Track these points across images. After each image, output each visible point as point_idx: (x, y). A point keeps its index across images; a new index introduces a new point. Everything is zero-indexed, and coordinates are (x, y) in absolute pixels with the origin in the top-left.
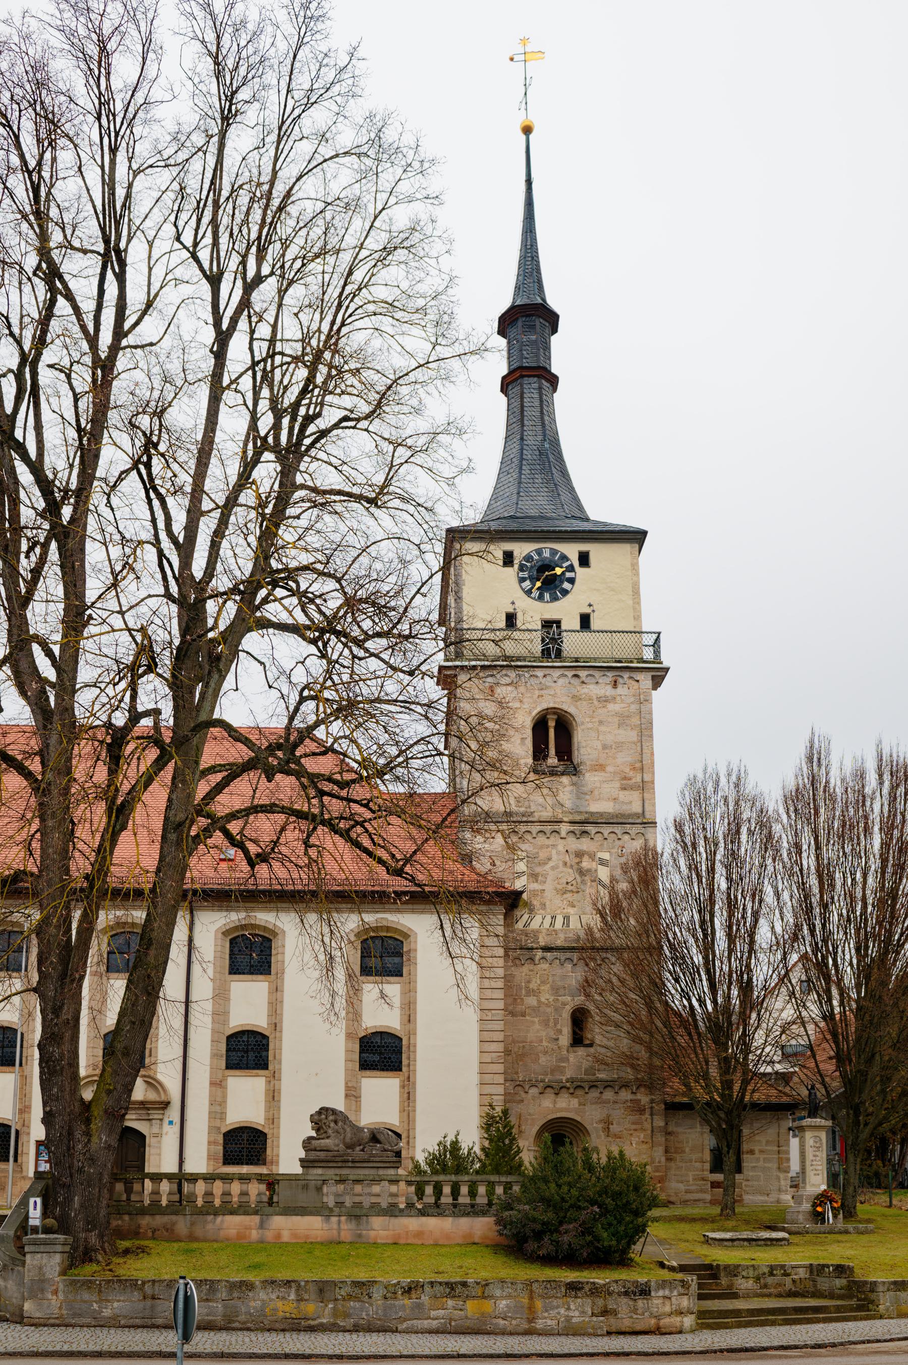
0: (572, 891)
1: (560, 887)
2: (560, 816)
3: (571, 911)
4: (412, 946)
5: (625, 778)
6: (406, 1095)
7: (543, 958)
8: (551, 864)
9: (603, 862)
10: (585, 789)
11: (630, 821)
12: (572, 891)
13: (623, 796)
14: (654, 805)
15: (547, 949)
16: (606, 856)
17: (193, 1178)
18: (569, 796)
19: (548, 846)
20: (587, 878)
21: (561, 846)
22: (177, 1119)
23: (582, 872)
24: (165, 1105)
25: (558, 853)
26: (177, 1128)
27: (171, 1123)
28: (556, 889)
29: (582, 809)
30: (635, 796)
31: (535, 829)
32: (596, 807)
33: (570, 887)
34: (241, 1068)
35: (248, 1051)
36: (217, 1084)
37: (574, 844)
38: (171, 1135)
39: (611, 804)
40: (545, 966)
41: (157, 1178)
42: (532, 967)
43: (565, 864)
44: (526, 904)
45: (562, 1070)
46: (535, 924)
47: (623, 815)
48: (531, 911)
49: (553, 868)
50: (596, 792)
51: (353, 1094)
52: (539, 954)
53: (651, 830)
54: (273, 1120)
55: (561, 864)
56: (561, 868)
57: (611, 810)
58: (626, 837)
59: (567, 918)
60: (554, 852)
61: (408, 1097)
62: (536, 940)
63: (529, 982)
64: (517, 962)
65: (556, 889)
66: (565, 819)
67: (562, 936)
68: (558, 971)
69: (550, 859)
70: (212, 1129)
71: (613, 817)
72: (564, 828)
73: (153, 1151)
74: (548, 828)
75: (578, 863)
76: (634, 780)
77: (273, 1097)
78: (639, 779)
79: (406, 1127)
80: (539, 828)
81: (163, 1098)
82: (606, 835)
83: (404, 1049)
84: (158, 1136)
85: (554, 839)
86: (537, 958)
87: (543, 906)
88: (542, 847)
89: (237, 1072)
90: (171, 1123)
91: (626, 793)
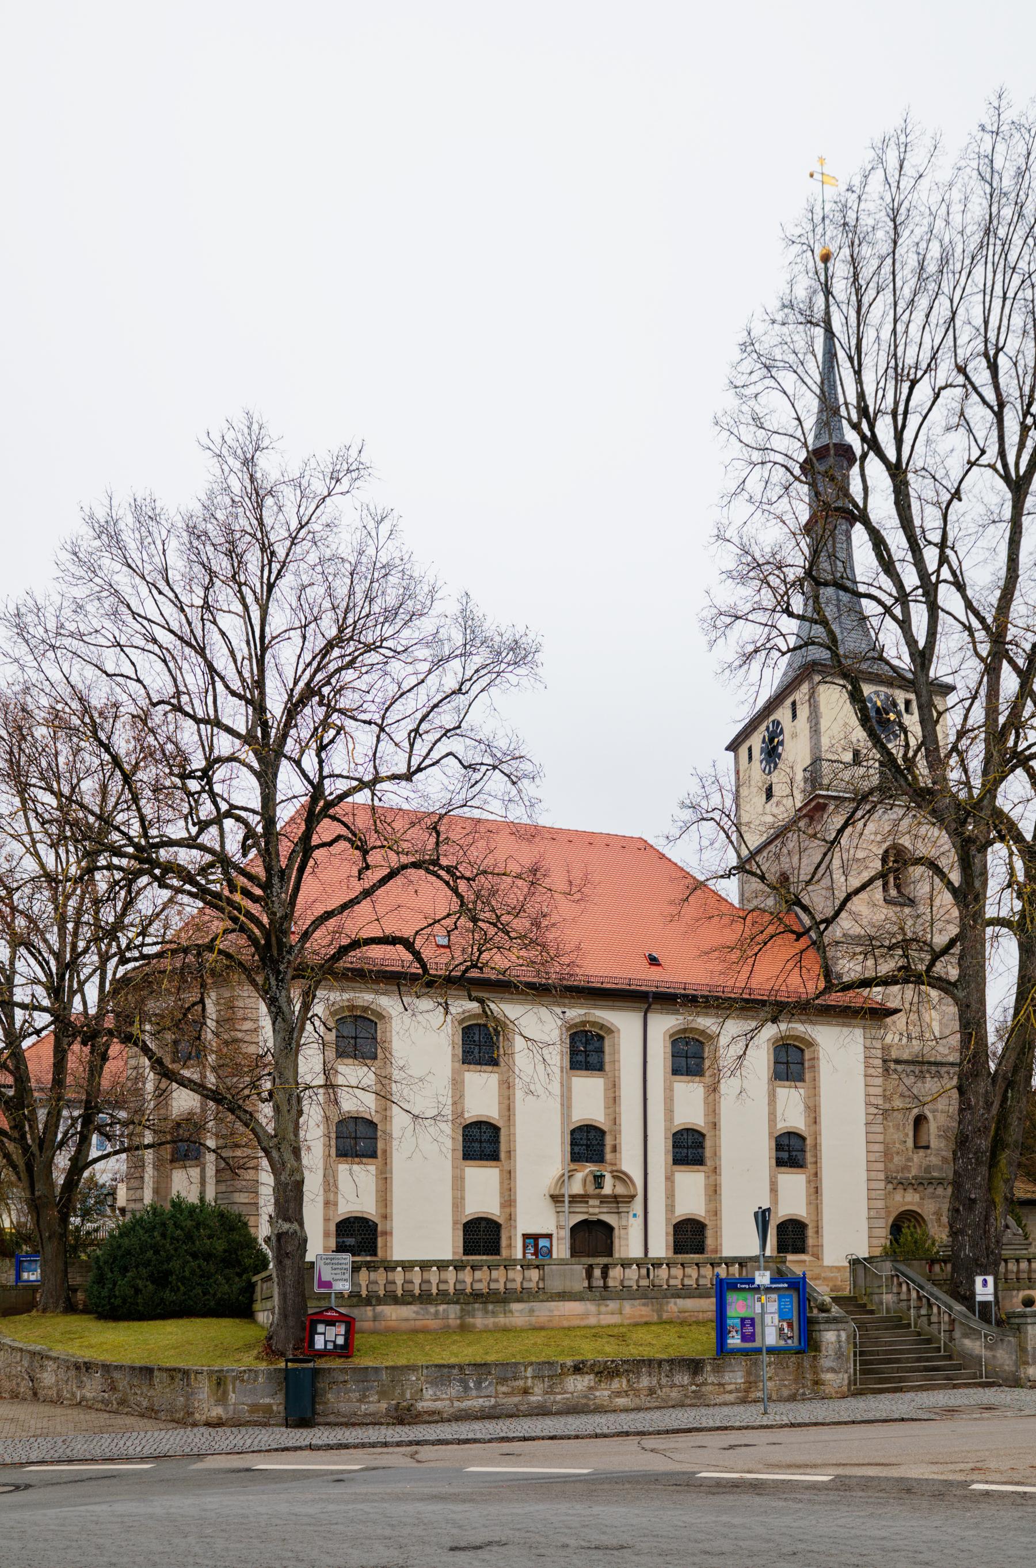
6: (813, 1190)
17: (657, 1264)
22: (640, 1212)
24: (633, 1197)
26: (640, 1220)
27: (635, 1215)
34: (688, 1164)
35: (690, 1148)
36: (669, 1179)
38: (635, 1226)
41: (626, 1264)
45: (906, 1168)
51: (774, 1190)
54: (716, 1213)
61: (815, 1191)
70: (668, 1220)
73: (623, 1242)
77: (714, 1191)
79: (814, 1218)
81: (633, 1193)
83: (808, 1148)
84: (625, 1228)
89: (682, 1168)
90: (635, 1215)
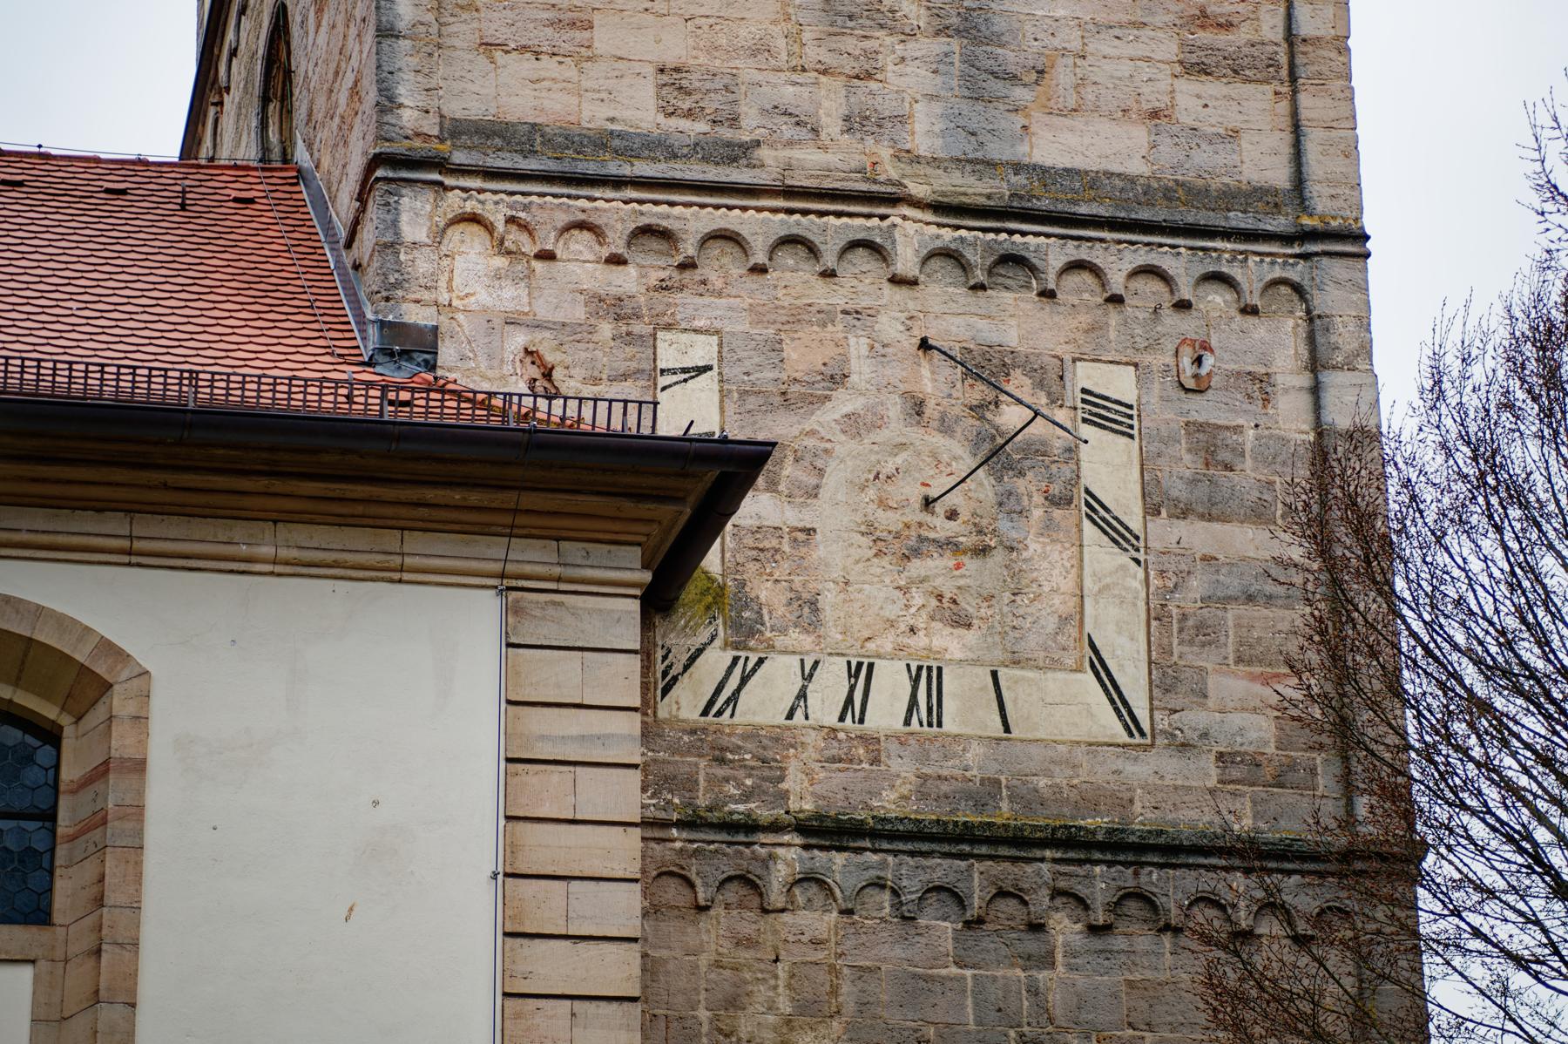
0: (950, 545)
1: (889, 520)
2: (890, 170)
3: (950, 644)
4: (122, 743)
5: (1203, 19)
7: (810, 879)
8: (844, 403)
9: (1103, 413)
10: (1009, 57)
11: (1237, 220)
12: (950, 545)
13: (1194, 100)
14: (1351, 152)
15: (828, 831)
16: (1120, 384)
18: (931, 83)
19: (826, 317)
20: (1028, 486)
21: (894, 318)
23: (997, 454)
25: (879, 351)
28: (869, 529)
29: (997, 150)
30: (1256, 106)
31: (759, 224)
32: (1060, 145)
33: (941, 527)
37: (952, 313)
39: (1139, 135)
40: (819, 921)
42: (748, 922)
43: (917, 408)
44: (716, 597)
46: (764, 702)
47: (1196, 194)
48: (746, 631)
49: (854, 424)
50: (1063, 76)
52: (789, 857)
53: (1338, 268)
55: (894, 408)
56: (896, 426)
57: (1136, 167)
58: (1217, 299)
59: (927, 679)
60: (858, 346)
62: (771, 771)
63: (734, 1003)
64: (672, 892)
65: (869, 529)
66: (918, 190)
67: (903, 767)
68: (888, 951)
69: (838, 379)
71: (1149, 196)
72: (912, 235)
74: (831, 230)
75: (978, 410)
76: (1243, 35)
78: (1271, 26)
80: (782, 224)
82: (1117, 281)
85: (860, 281)
86: (780, 873)
87: (808, 609)
88: (796, 318)
91: (1211, 88)
